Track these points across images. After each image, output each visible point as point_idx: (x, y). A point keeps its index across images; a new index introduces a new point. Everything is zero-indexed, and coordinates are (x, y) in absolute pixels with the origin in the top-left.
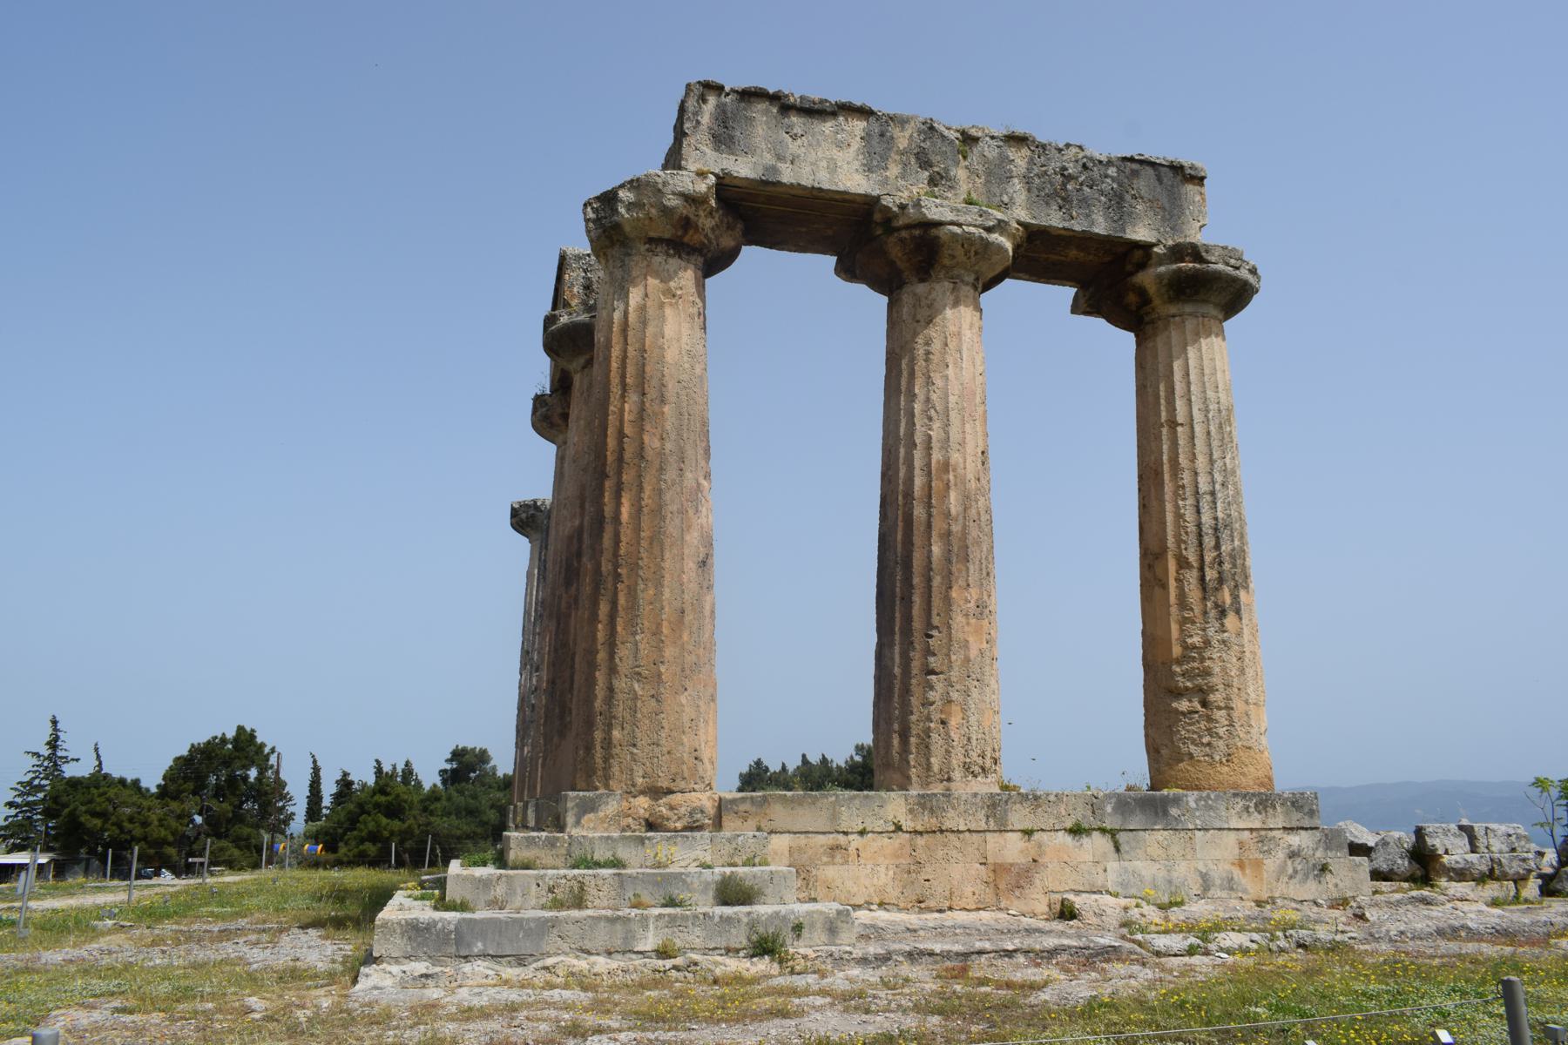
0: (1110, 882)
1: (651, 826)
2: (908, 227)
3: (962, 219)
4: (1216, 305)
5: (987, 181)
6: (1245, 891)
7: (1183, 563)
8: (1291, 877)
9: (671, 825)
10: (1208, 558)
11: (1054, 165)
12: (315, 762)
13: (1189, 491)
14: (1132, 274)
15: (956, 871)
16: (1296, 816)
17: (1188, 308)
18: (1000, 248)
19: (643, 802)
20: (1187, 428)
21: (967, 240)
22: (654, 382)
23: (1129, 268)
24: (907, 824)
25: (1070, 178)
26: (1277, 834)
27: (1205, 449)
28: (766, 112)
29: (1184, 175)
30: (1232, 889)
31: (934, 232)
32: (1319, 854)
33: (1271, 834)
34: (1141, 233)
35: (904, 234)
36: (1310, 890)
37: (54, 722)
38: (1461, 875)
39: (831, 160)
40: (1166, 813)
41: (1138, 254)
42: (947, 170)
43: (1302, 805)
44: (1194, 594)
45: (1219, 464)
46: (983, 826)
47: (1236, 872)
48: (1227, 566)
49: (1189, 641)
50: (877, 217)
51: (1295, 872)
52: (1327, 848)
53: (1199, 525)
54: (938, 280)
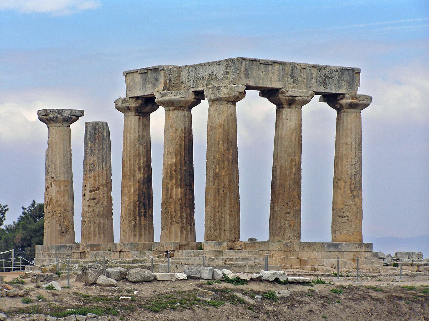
0: (326, 262)
1: (230, 249)
2: (288, 96)
3: (302, 95)
5: (307, 81)
7: (346, 183)
9: (235, 248)
10: (352, 182)
11: (323, 73)
13: (349, 163)
14: (339, 100)
17: (353, 110)
19: (229, 243)
20: (350, 145)
22: (230, 141)
23: (338, 98)
24: (282, 249)
25: (327, 77)
26: (363, 253)
27: (354, 152)
28: (256, 65)
29: (355, 73)
31: (295, 98)
33: (361, 253)
35: (287, 97)
36: (369, 266)
38: (405, 265)
39: (271, 78)
40: (338, 247)
41: (341, 96)
42: (297, 78)
43: (369, 245)
44: (349, 192)
45: (357, 156)
46: (298, 250)
47: (353, 263)
48: (357, 184)
49: (346, 204)
50: (280, 92)
53: (351, 173)
54: (293, 108)
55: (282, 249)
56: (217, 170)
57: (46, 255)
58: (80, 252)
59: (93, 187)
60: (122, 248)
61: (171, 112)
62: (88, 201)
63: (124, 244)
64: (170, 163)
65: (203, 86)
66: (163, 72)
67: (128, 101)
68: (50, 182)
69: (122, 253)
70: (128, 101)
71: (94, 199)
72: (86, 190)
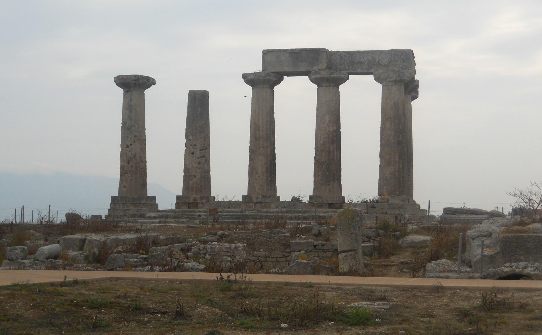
56: (400, 138)
57: (129, 205)
58: (189, 203)
59: (203, 147)
60: (260, 200)
61: (331, 88)
62: (198, 158)
63: (264, 197)
64: (331, 129)
65: (363, 69)
66: (325, 53)
67: (270, 75)
68: (133, 141)
69: (257, 205)
70: (270, 75)
71: (204, 157)
72: (196, 148)
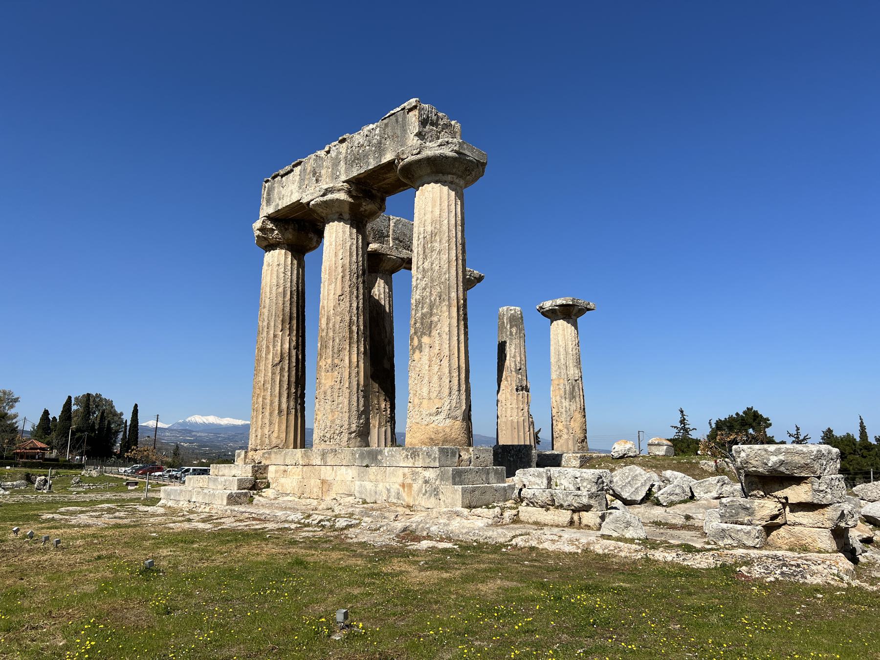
4: (428, 175)
6: (404, 500)
8: (424, 495)
12: (862, 423)
15: (312, 481)
16: (428, 460)
18: (332, 201)
21: (317, 205)
24: (301, 462)
30: (398, 498)
32: (437, 483)
34: (388, 157)
37: (682, 412)
40: (376, 457)
47: (401, 489)
48: (418, 325)
51: (426, 491)
52: (442, 480)
55: (301, 462)
